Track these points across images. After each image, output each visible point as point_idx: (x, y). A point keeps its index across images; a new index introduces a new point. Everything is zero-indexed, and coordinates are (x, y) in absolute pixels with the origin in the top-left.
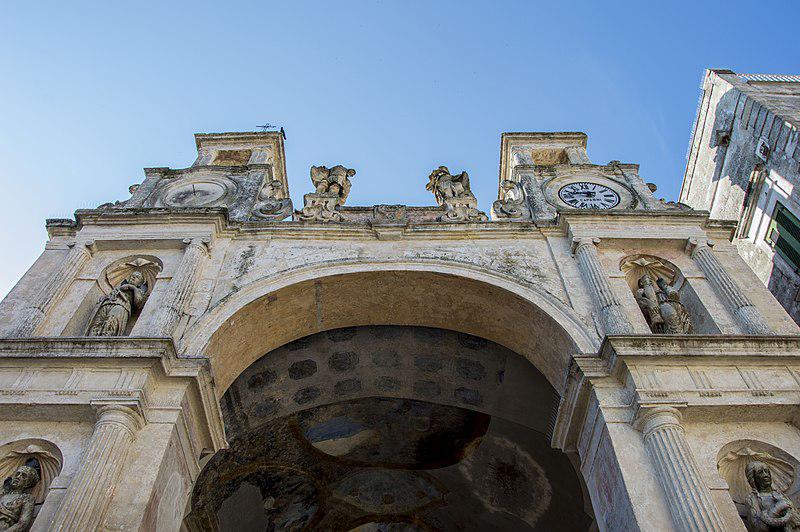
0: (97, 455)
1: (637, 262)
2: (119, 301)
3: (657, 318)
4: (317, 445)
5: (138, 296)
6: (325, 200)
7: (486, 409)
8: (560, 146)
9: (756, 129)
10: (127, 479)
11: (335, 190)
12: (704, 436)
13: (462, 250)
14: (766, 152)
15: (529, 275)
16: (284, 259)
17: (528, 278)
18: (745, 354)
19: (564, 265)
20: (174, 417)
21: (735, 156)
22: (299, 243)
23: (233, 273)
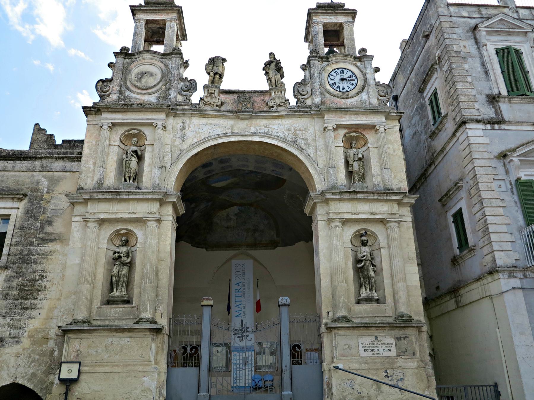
0: (152, 238)
1: (352, 134)
2: (133, 158)
3: (350, 169)
4: (214, 185)
5: (139, 153)
6: (214, 89)
7: (285, 177)
8: (340, 19)
9: (438, 45)
10: (161, 243)
11: (217, 76)
12: (350, 227)
13: (276, 127)
14: (439, 59)
15: (302, 143)
16: (199, 133)
17: (302, 146)
18: (372, 198)
19: (319, 137)
20: (171, 218)
21: (429, 48)
22: (204, 121)
23: (178, 141)
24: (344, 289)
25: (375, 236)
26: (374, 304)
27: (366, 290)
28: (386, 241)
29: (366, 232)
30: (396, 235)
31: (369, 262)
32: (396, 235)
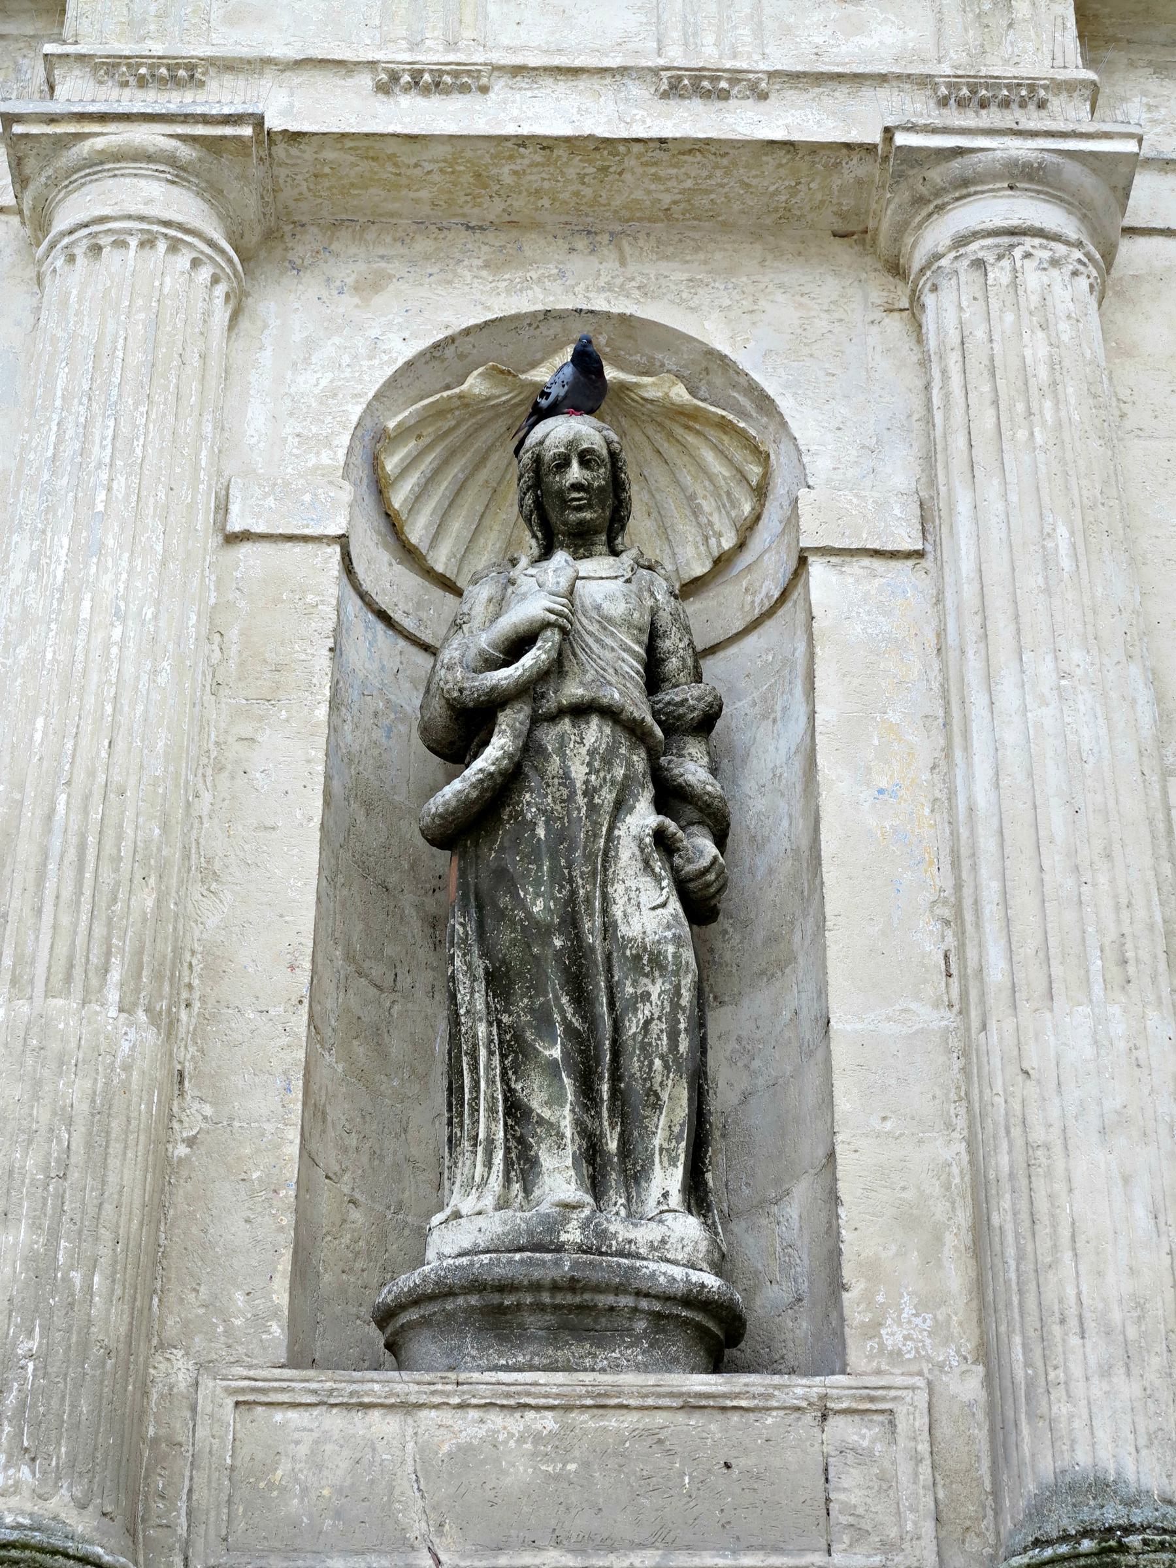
12: (370, 286)
24: (76, 1091)
25: (735, 419)
26: (645, 1384)
27: (523, 1165)
28: (900, 472)
29: (587, 362)
30: (1037, 349)
31: (595, 732)
32: (1037, 349)
